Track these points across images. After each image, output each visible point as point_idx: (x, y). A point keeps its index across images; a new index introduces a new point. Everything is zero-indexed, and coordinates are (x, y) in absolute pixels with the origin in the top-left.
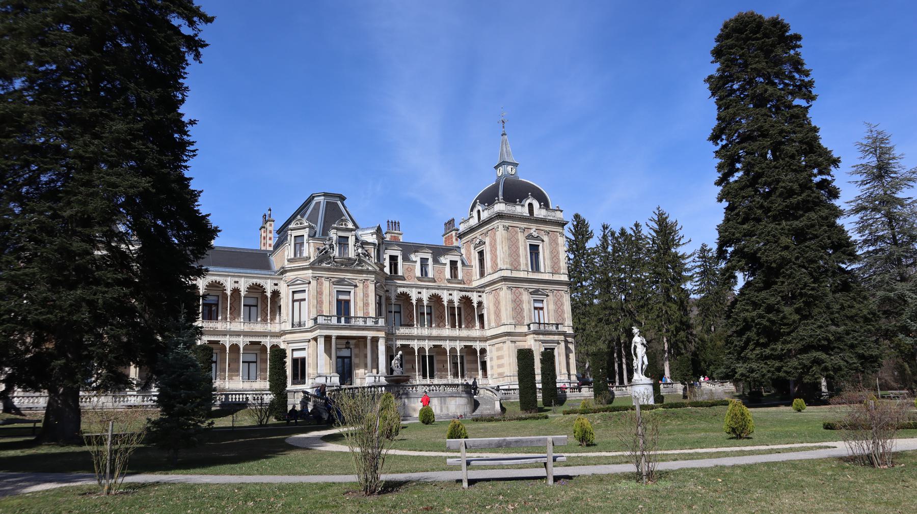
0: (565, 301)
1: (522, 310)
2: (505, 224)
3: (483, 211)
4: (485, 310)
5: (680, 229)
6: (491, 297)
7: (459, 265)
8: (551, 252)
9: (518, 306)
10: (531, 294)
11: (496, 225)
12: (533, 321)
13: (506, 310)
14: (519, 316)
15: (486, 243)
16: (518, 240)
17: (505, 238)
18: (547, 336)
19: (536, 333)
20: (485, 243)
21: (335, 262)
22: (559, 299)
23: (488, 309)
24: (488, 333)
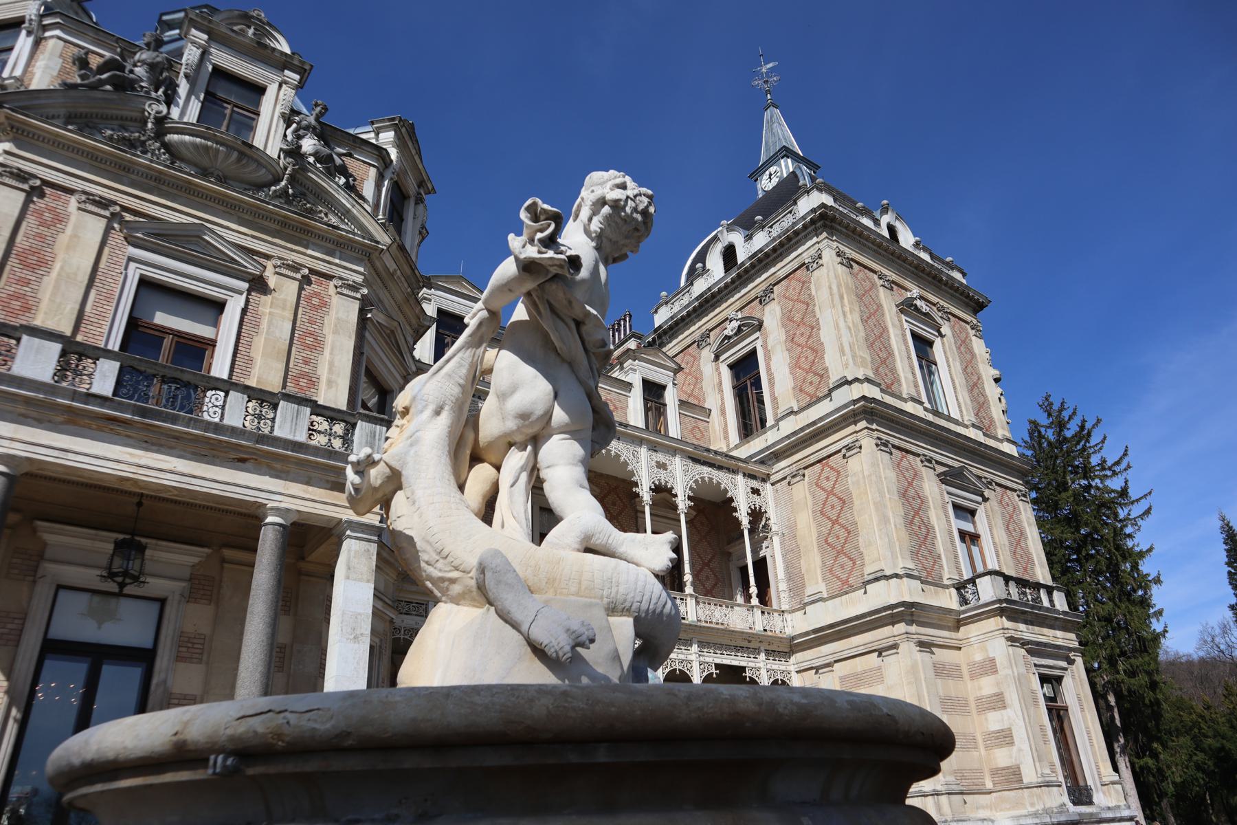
0: (1025, 525)
1: (929, 529)
2: (842, 248)
3: (749, 238)
4: (776, 540)
5: (1103, 442)
6: (801, 490)
7: (671, 398)
8: (965, 370)
9: (917, 513)
10: (943, 481)
11: (812, 251)
12: (980, 569)
13: (884, 520)
14: (923, 551)
15: (765, 324)
16: (880, 306)
17: (847, 287)
18: (1037, 629)
19: (1008, 610)
20: (760, 326)
21: (167, 146)
22: (1011, 517)
23: (791, 535)
24: (795, 625)
